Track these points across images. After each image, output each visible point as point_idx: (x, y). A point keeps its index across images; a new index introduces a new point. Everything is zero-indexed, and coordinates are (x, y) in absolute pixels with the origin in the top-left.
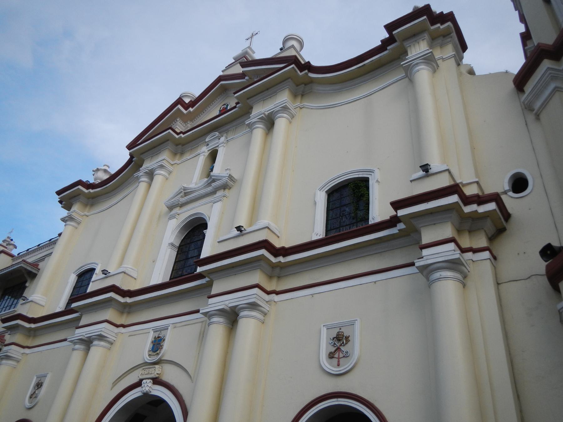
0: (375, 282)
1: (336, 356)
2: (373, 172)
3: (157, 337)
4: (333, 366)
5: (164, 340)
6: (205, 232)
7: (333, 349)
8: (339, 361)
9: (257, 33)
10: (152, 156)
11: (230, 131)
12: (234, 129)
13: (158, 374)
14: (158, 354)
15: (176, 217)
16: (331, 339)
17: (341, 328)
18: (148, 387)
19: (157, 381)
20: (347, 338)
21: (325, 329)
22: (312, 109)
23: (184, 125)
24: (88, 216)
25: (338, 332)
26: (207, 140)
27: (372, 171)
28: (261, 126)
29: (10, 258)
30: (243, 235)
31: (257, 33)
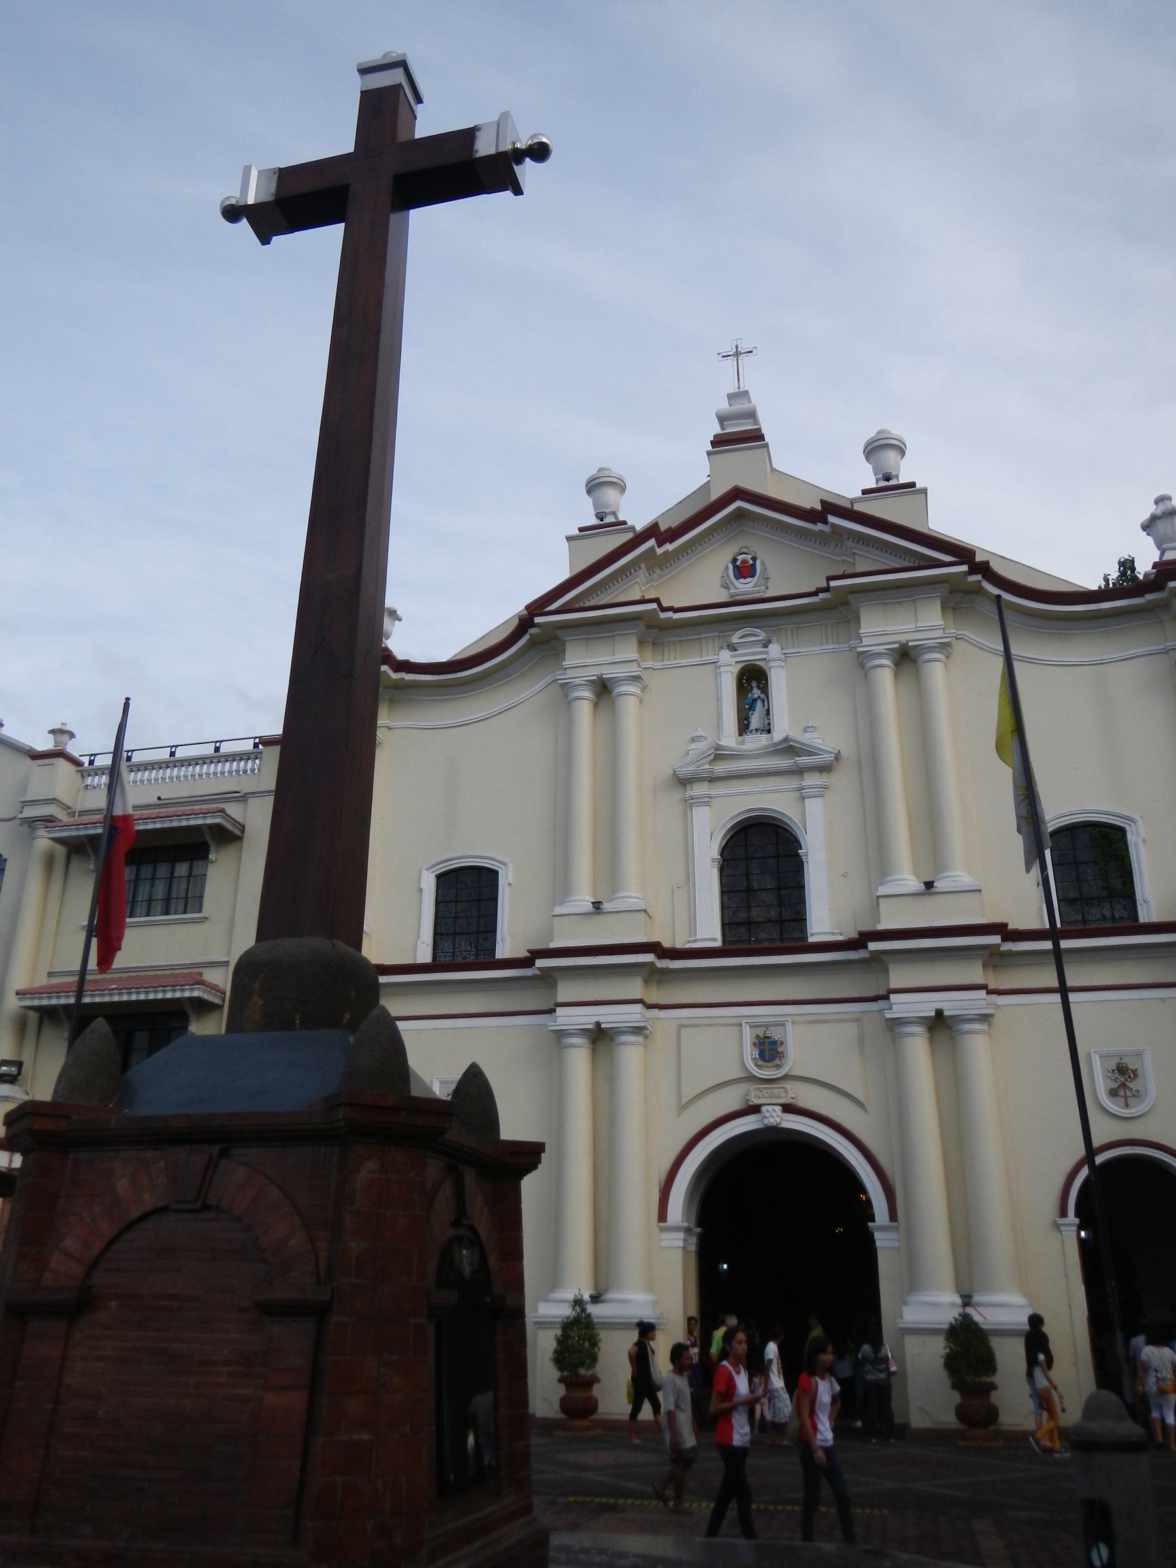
0: (1163, 1000)
1: (1121, 1093)
2: (1134, 822)
3: (762, 1036)
4: (1119, 1107)
5: (782, 1043)
6: (801, 854)
7: (1115, 1085)
8: (1126, 1101)
9: (751, 352)
10: (587, 639)
11: (783, 632)
12: (792, 630)
13: (793, 1098)
14: (778, 1066)
15: (710, 804)
16: (1109, 1071)
17: (1122, 1057)
18: (774, 1116)
19: (788, 1108)
20: (1134, 1072)
21: (1097, 1057)
22: (981, 648)
23: (648, 575)
24: (390, 728)
25: (1119, 1064)
26: (735, 639)
27: (1132, 820)
28: (886, 662)
29: (72, 768)
30: (931, 894)
31: (751, 352)
